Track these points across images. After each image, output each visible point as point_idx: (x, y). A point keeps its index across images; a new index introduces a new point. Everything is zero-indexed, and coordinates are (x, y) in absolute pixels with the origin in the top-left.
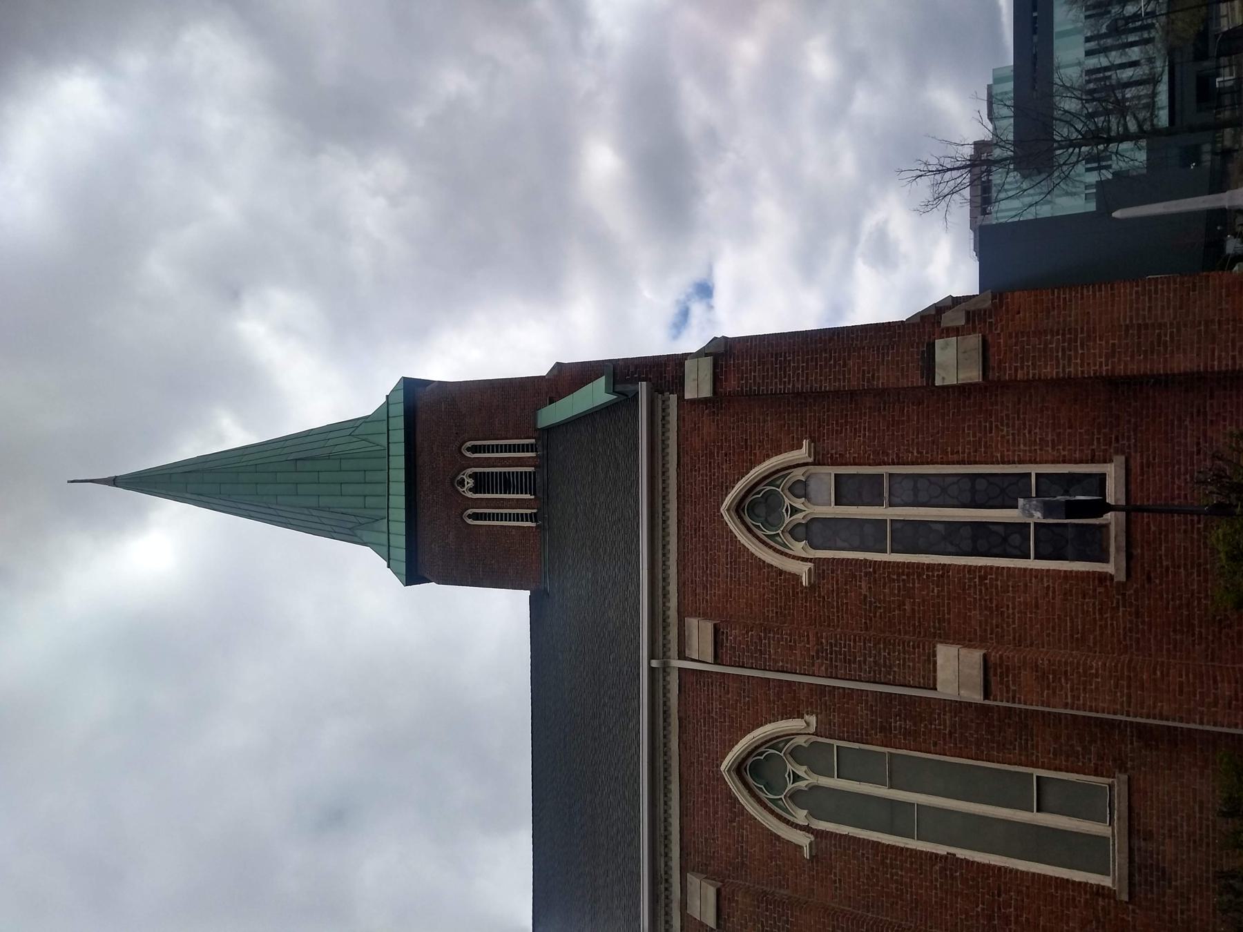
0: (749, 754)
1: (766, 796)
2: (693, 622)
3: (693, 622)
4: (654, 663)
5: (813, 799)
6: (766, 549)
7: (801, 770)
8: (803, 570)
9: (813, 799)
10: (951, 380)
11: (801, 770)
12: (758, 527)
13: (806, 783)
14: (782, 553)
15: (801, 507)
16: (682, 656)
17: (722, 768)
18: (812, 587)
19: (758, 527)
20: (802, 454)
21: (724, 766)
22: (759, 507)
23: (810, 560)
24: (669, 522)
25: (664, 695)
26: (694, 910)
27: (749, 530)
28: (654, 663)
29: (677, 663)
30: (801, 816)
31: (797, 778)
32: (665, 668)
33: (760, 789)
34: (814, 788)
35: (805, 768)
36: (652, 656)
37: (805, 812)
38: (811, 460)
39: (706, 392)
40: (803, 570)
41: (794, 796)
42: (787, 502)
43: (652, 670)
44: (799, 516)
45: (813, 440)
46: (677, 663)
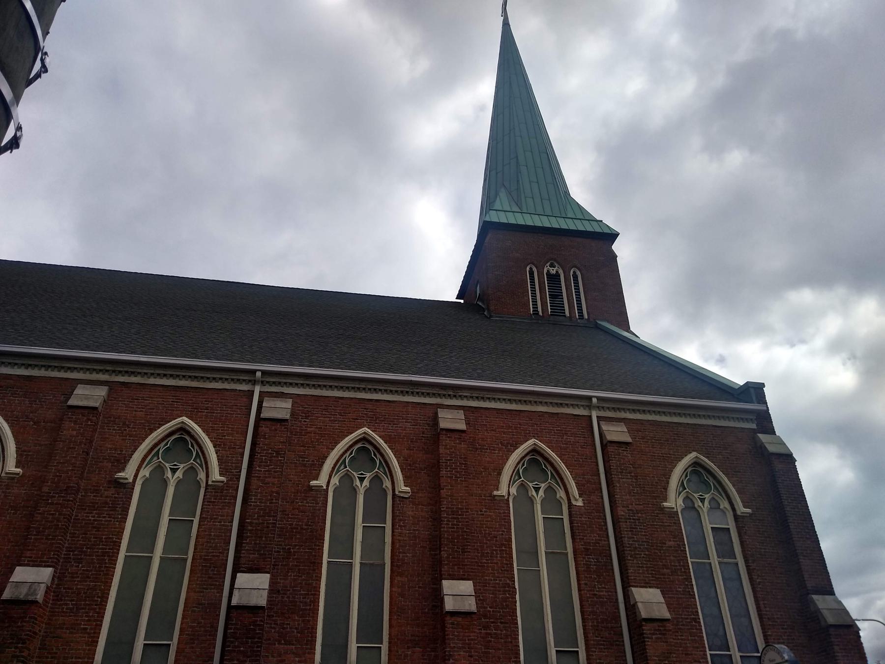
0: (192, 437)
1: (162, 448)
2: (288, 404)
3: (288, 404)
4: (259, 374)
5: (157, 482)
6: (337, 457)
7: (179, 474)
8: (321, 481)
9: (157, 482)
10: (446, 591)
11: (179, 474)
12: (351, 453)
14: (333, 468)
15: (364, 485)
16: (262, 395)
17: (184, 418)
18: (311, 488)
19: (351, 453)
21: (185, 419)
22: (365, 452)
23: (327, 488)
26: (80, 390)
27: (351, 446)
28: (259, 374)
29: (257, 390)
30: (145, 472)
31: (174, 471)
32: (254, 382)
33: (166, 444)
34: (165, 483)
35: (181, 477)
36: (264, 373)
37: (148, 475)
39: (443, 425)
40: (321, 481)
41: (160, 469)
43: (254, 372)
44: (358, 483)
46: (257, 390)
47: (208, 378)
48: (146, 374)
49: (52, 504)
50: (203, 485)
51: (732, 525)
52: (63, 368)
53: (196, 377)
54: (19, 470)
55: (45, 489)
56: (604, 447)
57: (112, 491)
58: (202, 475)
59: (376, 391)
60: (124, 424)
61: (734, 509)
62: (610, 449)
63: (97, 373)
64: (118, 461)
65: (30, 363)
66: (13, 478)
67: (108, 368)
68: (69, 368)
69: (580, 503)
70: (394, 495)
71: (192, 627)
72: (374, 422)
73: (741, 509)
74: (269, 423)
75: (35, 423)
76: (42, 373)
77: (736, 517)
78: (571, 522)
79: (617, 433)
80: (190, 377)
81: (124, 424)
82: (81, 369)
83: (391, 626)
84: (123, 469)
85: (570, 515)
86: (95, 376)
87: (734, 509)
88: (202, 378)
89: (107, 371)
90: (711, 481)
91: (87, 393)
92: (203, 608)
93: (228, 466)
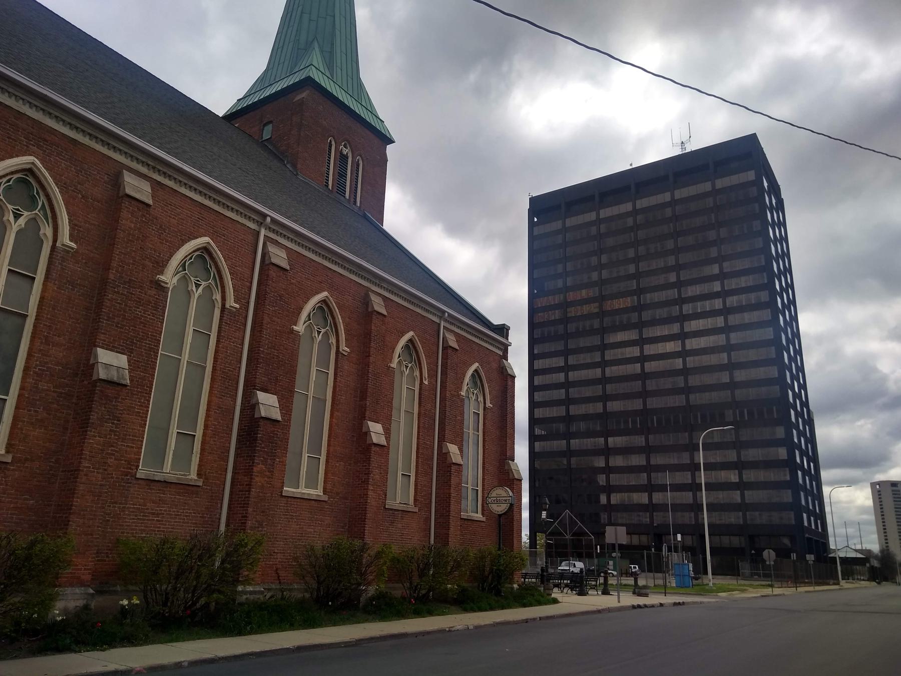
4: (269, 219)
13: (13, 222)
20: (65, 238)
24: (203, 198)
25: (70, 124)
29: (263, 232)
34: (189, 294)
38: (58, 244)
42: (26, 213)
43: (265, 216)
45: (77, 251)
47: (228, 206)
48: (180, 182)
49: (118, 292)
50: (219, 305)
51: (481, 412)
52: (108, 144)
53: (219, 202)
54: (73, 245)
55: (111, 276)
56: (444, 348)
57: (153, 292)
58: (218, 296)
59: (336, 263)
60: (161, 227)
61: (485, 403)
62: (450, 351)
63: (138, 163)
64: (157, 263)
65: (78, 125)
66: (68, 252)
67: (150, 163)
68: (114, 148)
69: (426, 383)
70: (54, 247)
71: (214, 425)
72: (331, 288)
73: (489, 405)
74: (275, 268)
75: (83, 196)
76: (86, 141)
77: (485, 408)
78: (420, 394)
79: (279, 257)
80: (214, 199)
81: (161, 227)
82: (126, 153)
83: (329, 445)
84: (162, 273)
85: (420, 389)
86: (144, 170)
87: (485, 403)
88: (224, 204)
89: (148, 165)
90: (330, 319)
91: (136, 183)
92: (218, 410)
93: (242, 297)
